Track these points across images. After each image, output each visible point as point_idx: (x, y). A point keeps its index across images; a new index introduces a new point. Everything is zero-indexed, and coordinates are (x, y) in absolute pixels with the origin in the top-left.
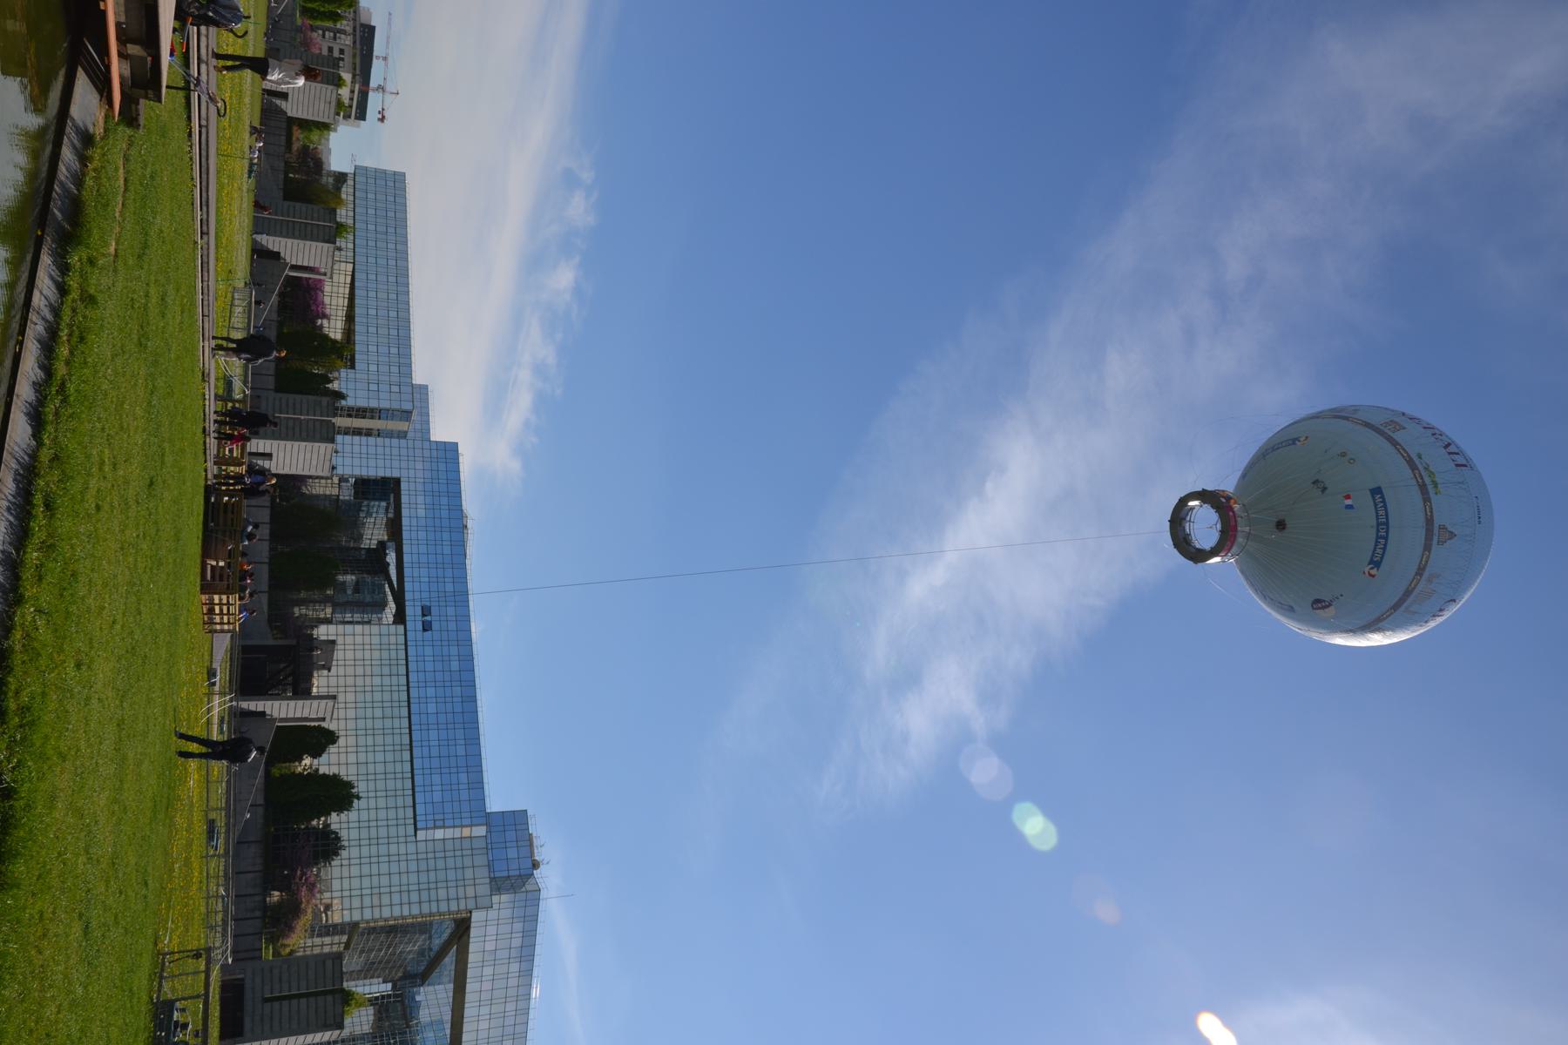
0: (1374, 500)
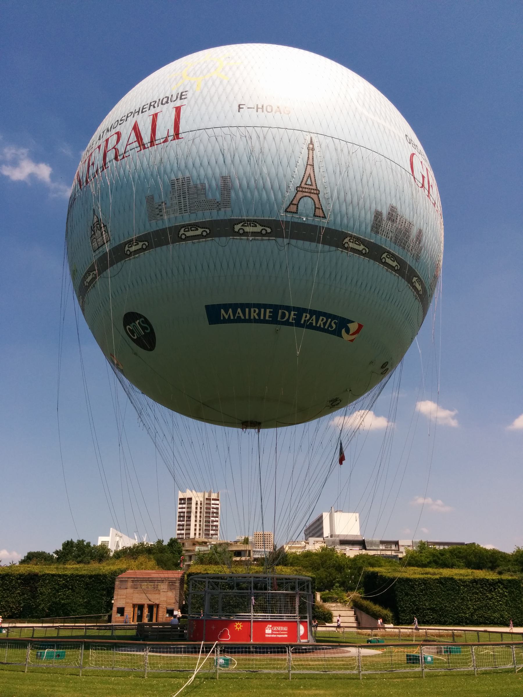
0: (225, 321)
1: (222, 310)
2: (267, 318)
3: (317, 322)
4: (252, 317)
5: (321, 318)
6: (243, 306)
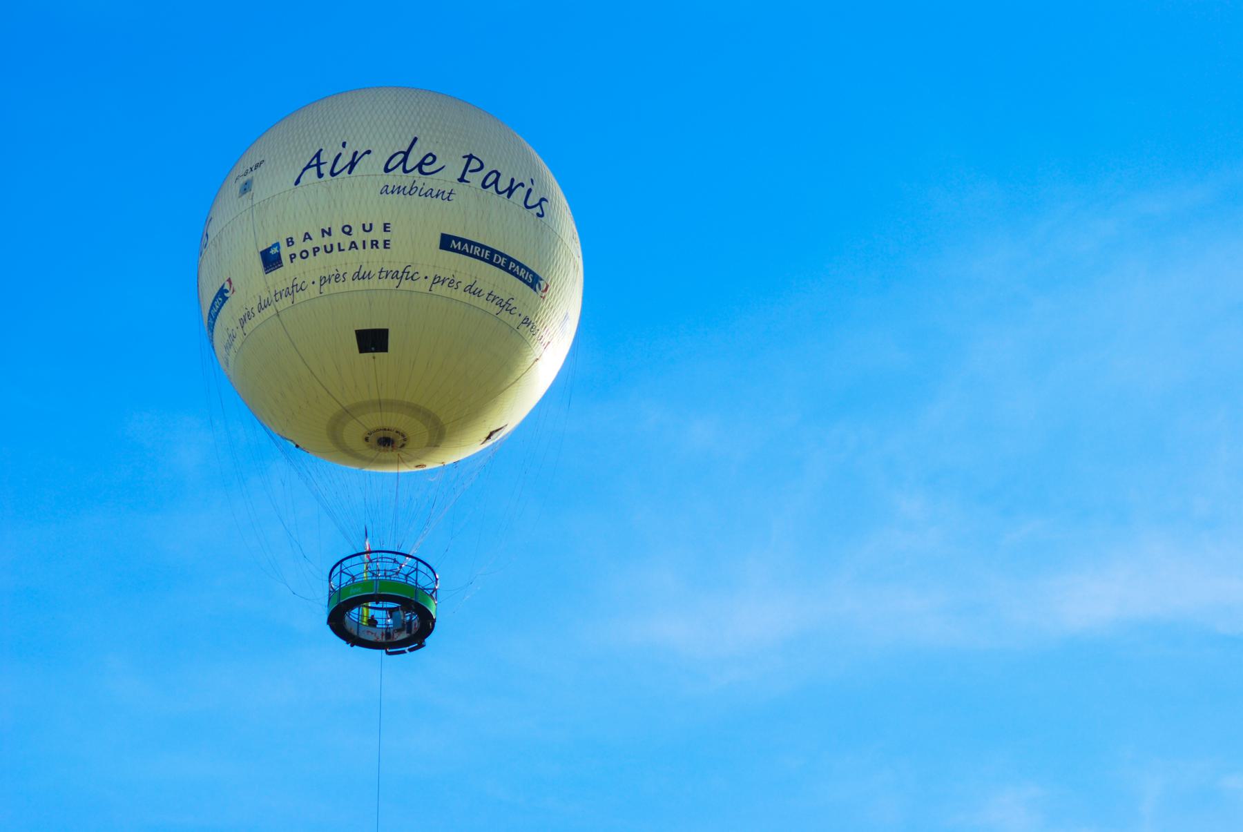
1: (453, 242)
2: (486, 257)
3: (520, 271)
4: (475, 253)
5: (522, 269)
6: (470, 243)
